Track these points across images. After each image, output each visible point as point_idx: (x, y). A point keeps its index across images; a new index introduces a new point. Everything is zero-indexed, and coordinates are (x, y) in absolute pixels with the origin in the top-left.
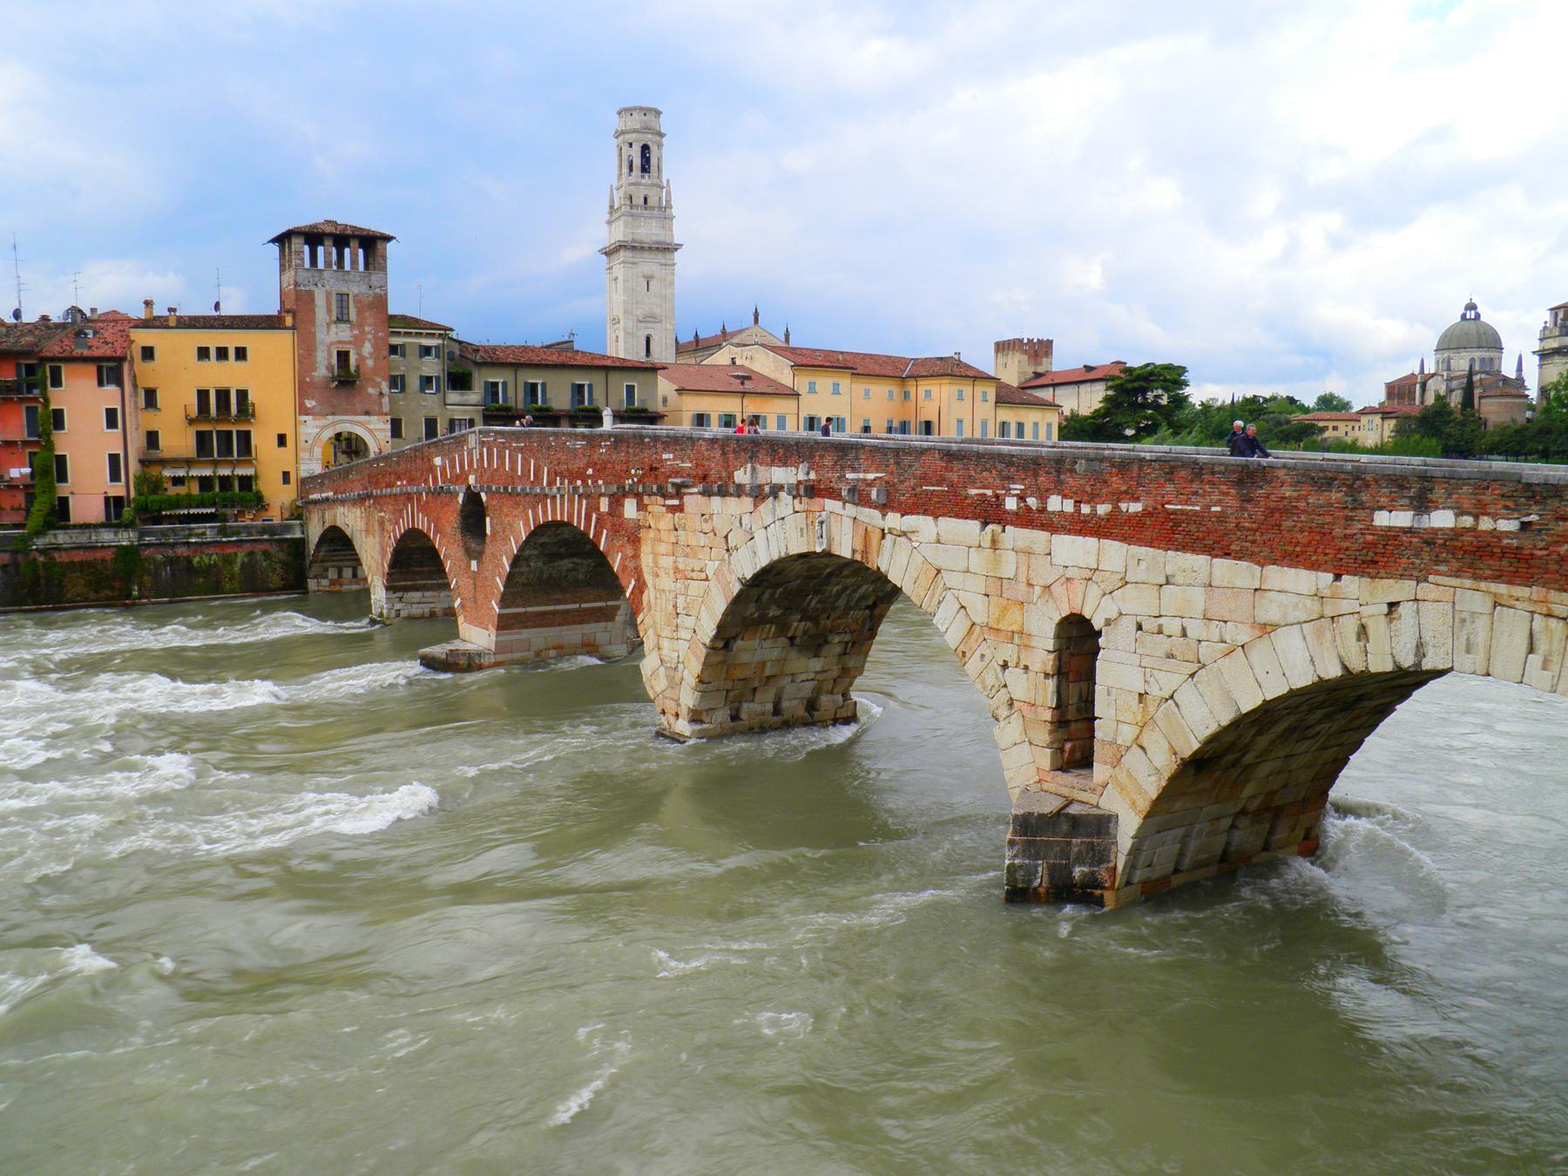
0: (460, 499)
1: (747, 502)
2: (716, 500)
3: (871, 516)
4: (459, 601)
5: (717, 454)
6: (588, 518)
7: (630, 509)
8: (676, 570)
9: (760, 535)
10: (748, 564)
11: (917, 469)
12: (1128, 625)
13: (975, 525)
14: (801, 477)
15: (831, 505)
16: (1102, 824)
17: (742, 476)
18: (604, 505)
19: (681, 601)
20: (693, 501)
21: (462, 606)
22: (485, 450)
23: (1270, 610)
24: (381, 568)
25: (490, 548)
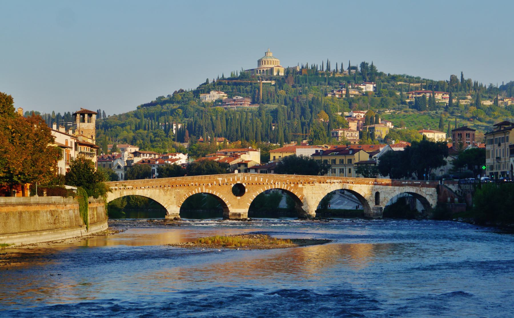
0: (233, 185)
1: (329, 184)
2: (322, 184)
3: (352, 185)
4: (230, 205)
5: (323, 179)
6: (287, 187)
7: (300, 186)
8: (313, 193)
9: (331, 188)
10: (329, 191)
11: (358, 180)
12: (383, 192)
13: (366, 185)
14: (340, 181)
15: (344, 184)
16: (382, 208)
17: (328, 181)
18: (292, 185)
19: (313, 197)
20: (317, 184)
21: (231, 206)
22: (246, 177)
23: (395, 190)
24: (175, 203)
25: (245, 195)
